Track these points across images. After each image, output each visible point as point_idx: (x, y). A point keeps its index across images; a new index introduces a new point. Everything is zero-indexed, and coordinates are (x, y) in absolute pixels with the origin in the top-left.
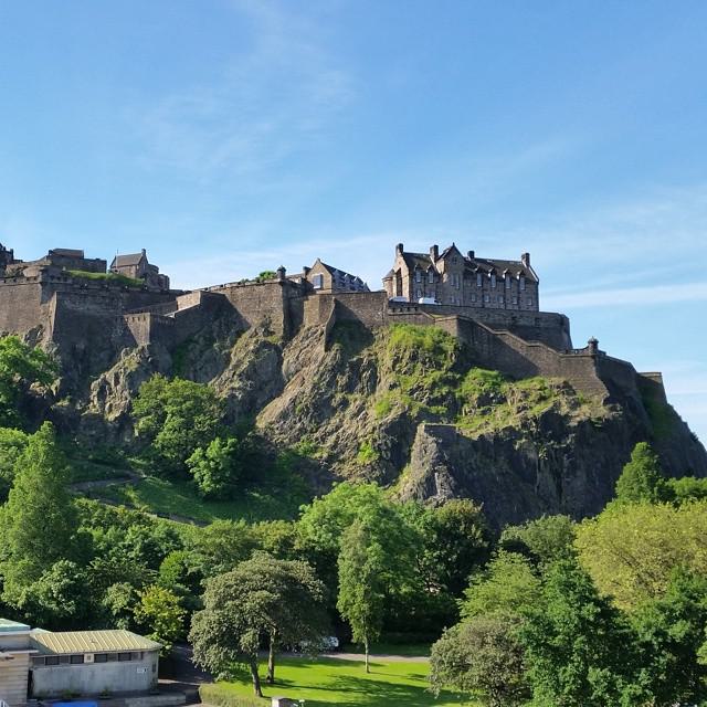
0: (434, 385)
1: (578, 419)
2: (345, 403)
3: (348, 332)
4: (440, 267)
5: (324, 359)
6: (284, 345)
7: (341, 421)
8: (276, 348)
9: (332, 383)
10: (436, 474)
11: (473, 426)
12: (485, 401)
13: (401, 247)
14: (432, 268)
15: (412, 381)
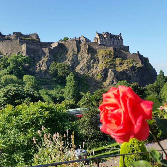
0: (110, 61)
1: (137, 67)
2: (93, 66)
3: (92, 51)
4: (105, 36)
5: (88, 57)
6: (78, 54)
7: (93, 70)
8: (76, 55)
9: (90, 62)
10: (114, 79)
11: (119, 69)
12: (120, 64)
13: (97, 32)
14: (104, 37)
15: (106, 60)
